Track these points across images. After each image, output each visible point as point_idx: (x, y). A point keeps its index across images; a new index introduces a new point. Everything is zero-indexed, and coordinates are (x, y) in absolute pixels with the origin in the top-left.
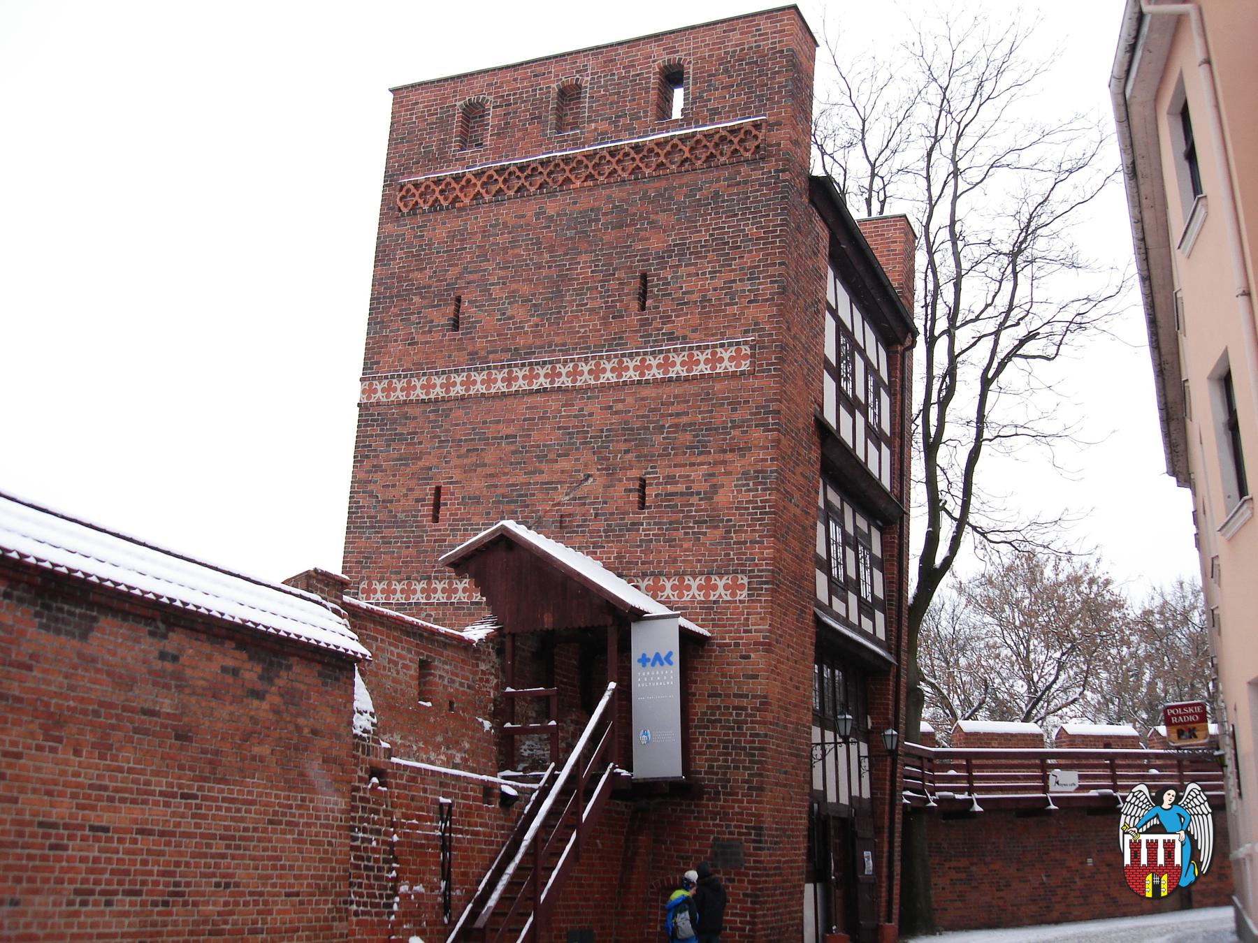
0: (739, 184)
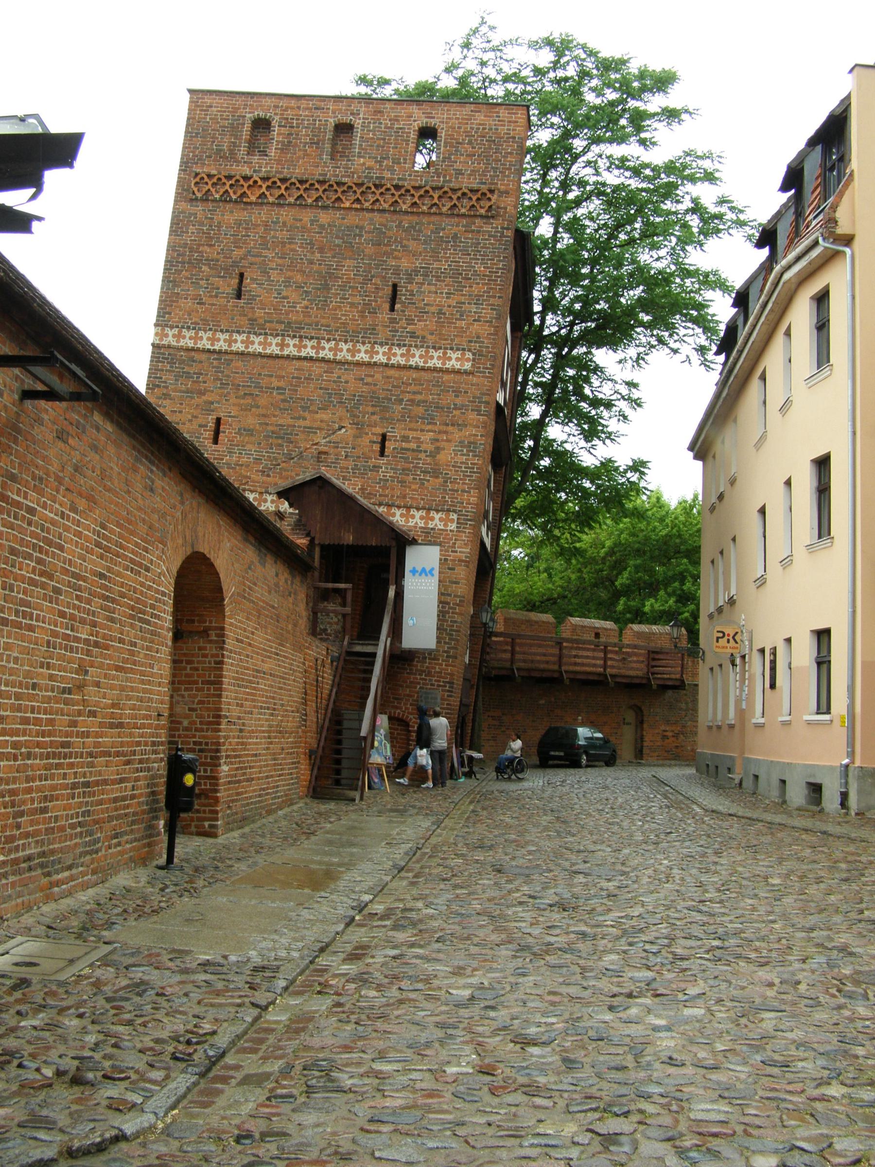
0: (473, 231)
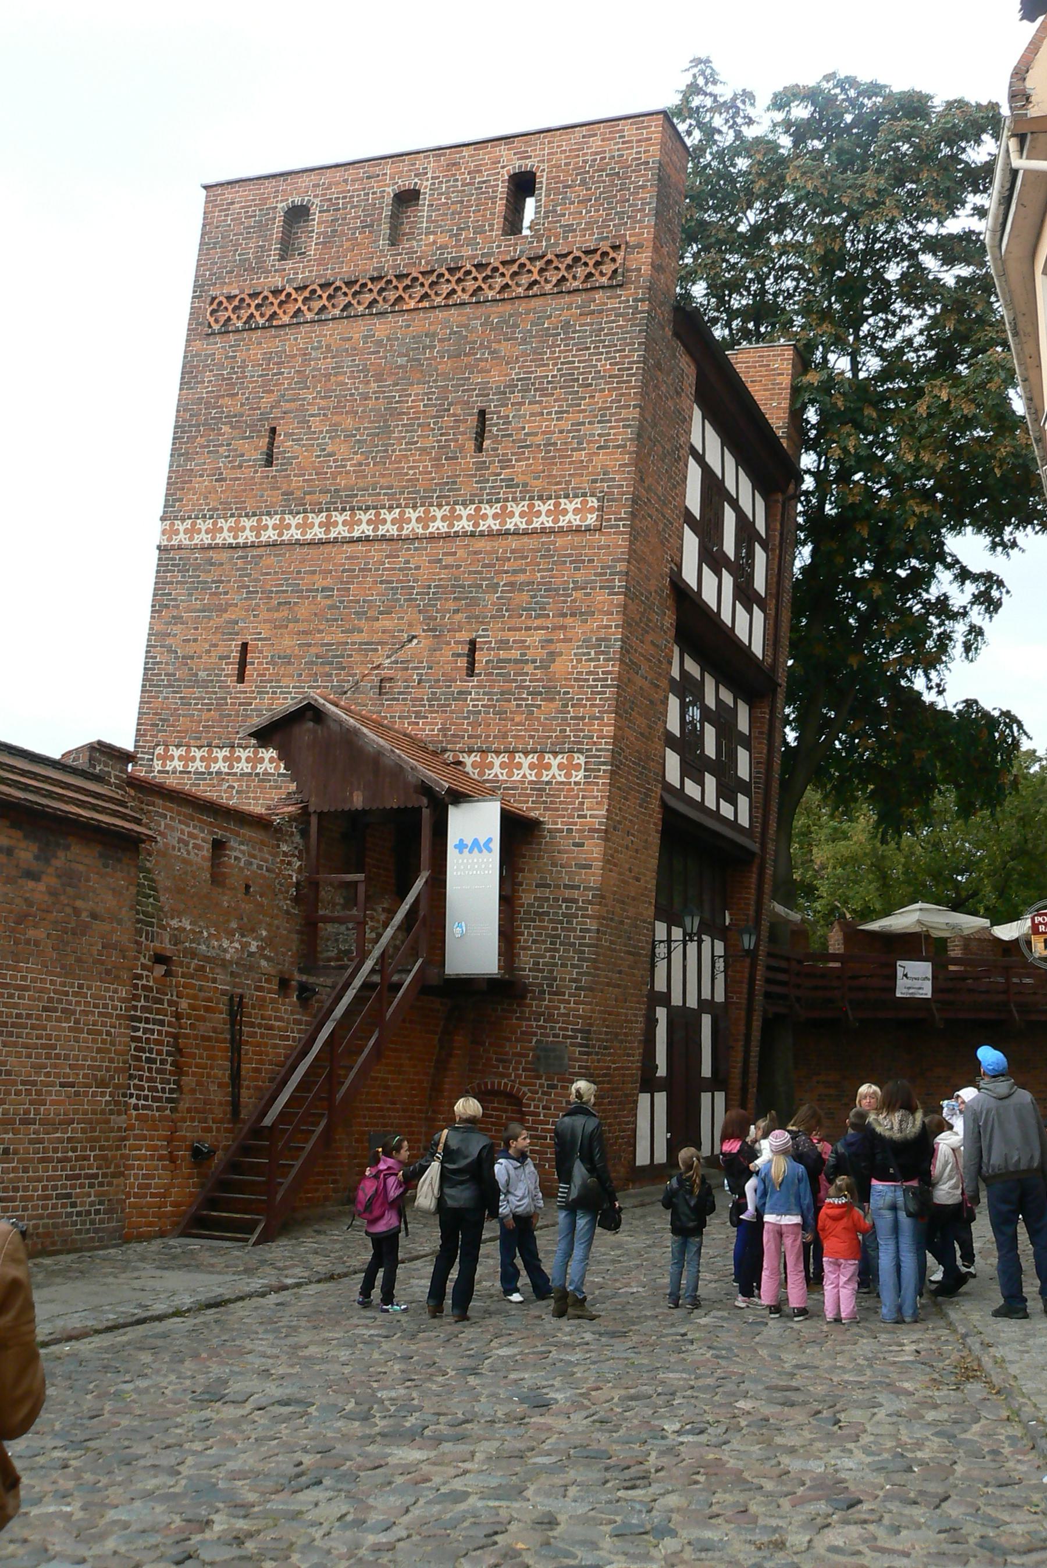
0: (592, 312)
